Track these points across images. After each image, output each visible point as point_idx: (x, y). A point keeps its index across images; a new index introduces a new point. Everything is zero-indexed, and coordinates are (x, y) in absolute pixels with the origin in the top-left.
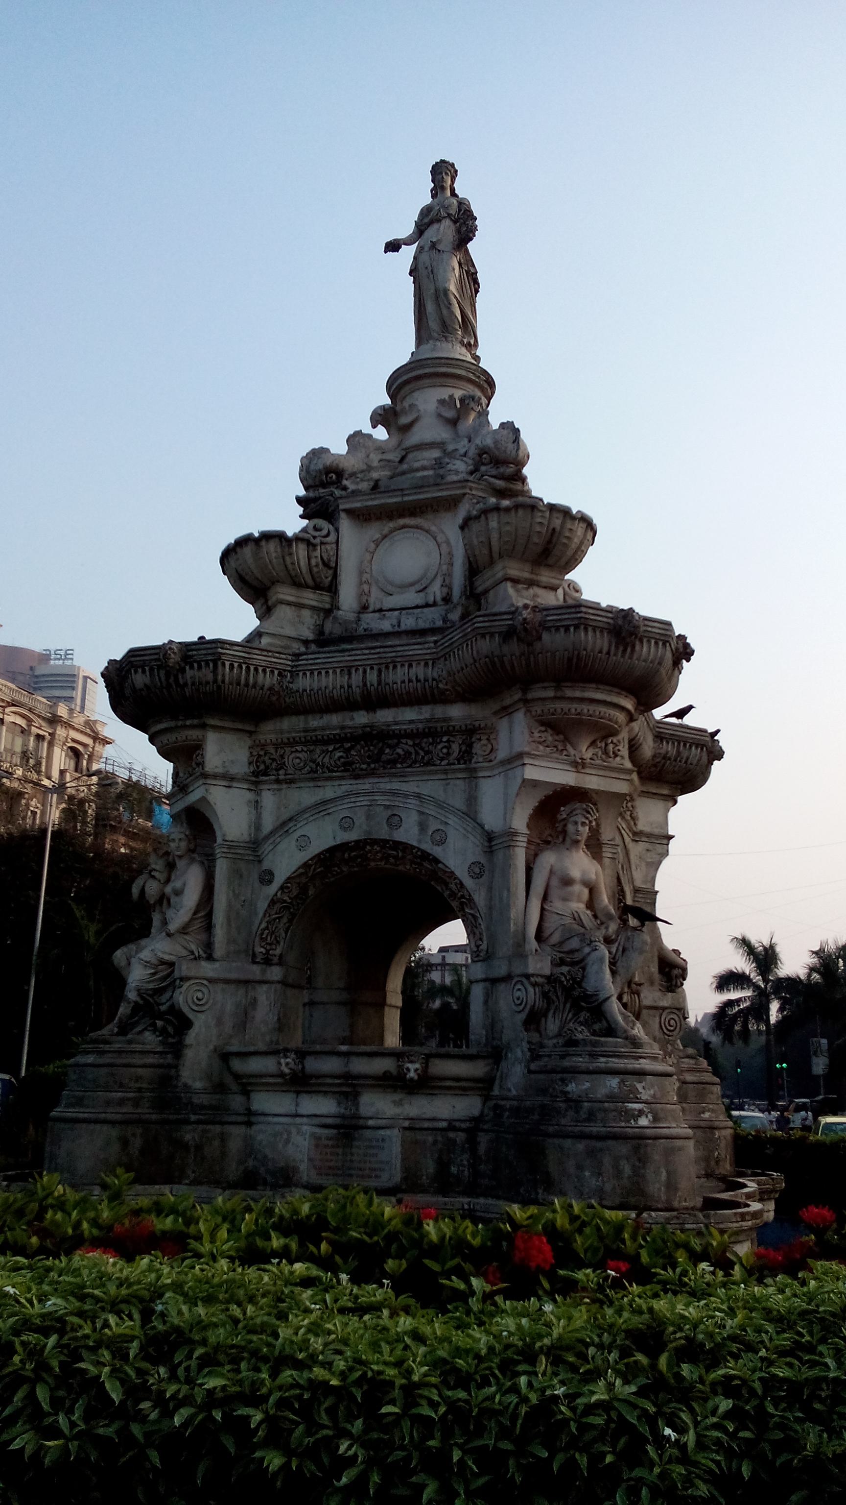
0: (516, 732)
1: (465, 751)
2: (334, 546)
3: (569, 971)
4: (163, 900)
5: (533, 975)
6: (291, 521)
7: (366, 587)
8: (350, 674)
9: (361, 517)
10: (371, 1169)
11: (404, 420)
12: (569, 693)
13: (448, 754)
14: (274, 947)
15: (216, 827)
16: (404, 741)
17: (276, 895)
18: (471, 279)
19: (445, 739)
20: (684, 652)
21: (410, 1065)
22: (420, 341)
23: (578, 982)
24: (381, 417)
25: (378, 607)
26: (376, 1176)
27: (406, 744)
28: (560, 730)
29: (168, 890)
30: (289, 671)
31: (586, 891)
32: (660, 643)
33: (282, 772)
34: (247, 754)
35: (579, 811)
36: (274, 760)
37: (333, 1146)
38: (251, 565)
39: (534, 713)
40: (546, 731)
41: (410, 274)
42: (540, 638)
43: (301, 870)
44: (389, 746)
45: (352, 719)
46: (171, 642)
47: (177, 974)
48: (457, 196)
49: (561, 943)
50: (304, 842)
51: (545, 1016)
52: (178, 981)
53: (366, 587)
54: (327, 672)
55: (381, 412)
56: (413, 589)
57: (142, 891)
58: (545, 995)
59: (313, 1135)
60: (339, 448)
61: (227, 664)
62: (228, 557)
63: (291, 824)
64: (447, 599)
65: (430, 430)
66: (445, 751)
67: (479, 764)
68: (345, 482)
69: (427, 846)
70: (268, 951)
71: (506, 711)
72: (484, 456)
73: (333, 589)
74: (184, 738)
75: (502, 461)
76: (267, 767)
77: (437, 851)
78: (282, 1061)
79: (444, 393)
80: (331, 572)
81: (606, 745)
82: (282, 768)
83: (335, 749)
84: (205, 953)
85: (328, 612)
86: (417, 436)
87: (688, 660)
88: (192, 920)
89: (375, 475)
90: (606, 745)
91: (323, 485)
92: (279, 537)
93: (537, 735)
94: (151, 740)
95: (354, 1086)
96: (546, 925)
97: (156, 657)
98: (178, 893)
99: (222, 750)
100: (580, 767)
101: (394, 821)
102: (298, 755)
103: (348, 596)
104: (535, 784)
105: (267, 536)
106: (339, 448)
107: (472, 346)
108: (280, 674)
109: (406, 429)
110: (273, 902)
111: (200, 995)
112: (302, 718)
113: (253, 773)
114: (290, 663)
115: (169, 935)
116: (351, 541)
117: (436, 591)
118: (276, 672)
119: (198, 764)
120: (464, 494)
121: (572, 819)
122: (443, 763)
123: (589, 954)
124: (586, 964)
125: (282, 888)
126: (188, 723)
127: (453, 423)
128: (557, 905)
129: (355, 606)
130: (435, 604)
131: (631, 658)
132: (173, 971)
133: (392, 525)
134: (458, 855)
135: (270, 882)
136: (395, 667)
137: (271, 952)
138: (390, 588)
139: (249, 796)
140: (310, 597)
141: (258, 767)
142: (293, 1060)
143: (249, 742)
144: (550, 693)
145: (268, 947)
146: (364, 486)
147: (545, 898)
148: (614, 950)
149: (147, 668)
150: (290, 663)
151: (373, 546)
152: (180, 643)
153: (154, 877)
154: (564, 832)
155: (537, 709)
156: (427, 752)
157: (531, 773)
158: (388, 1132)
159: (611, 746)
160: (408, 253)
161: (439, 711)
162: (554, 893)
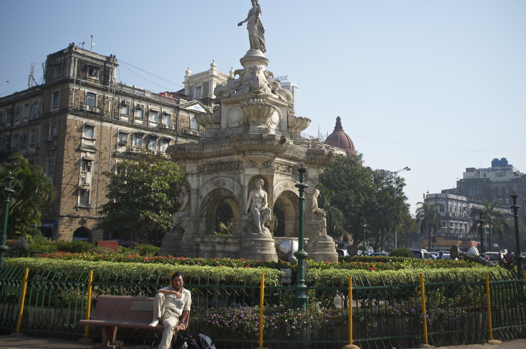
69: (231, 190)
101: (224, 184)
110: (202, 203)
130: (242, 126)
133: (233, 106)
160: (245, 25)
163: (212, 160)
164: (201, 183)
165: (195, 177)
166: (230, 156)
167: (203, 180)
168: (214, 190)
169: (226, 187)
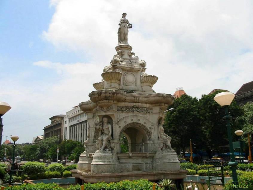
50: (125, 122)
77: (145, 125)
101: (139, 120)
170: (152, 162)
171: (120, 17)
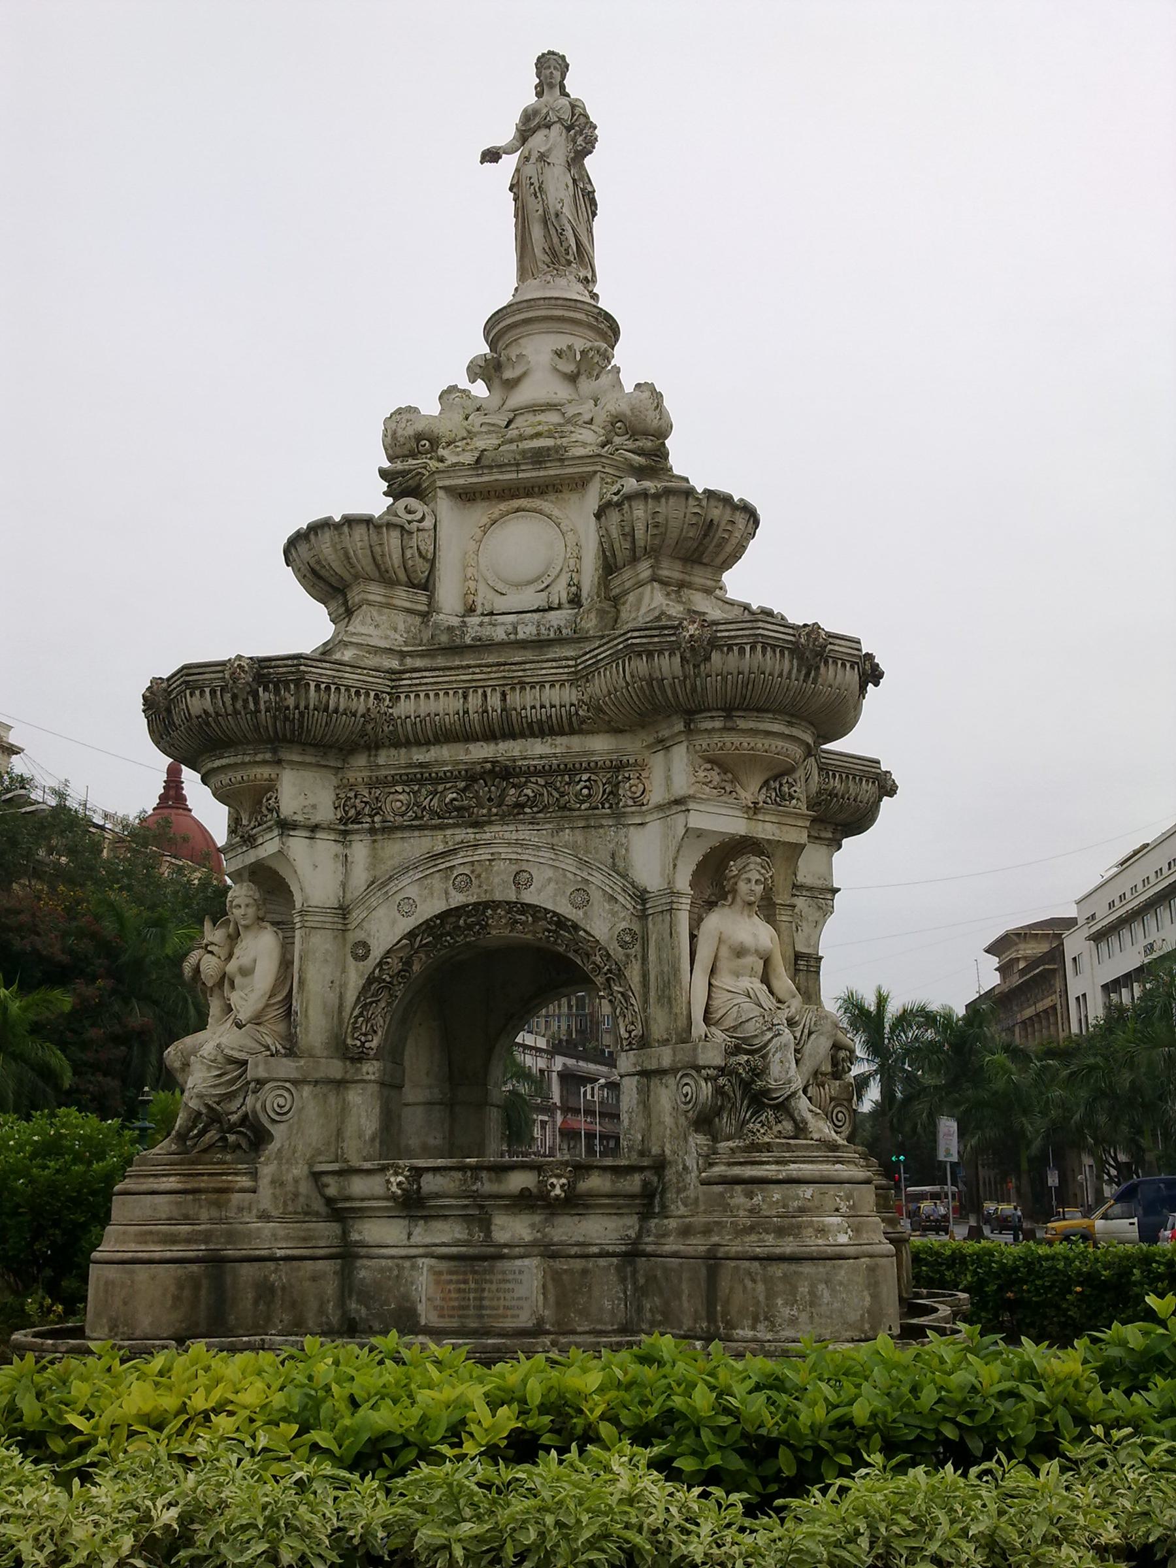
0: (674, 771)
1: (611, 793)
2: (432, 533)
3: (748, 1061)
4: (224, 981)
5: (704, 1068)
6: (374, 501)
7: (472, 584)
8: (465, 697)
9: (463, 497)
10: (506, 1308)
11: (508, 374)
12: (742, 724)
13: (589, 795)
14: (370, 1037)
15: (294, 889)
16: (533, 779)
17: (373, 972)
18: (587, 200)
19: (585, 777)
20: (871, 674)
21: (554, 1180)
22: (524, 273)
23: (759, 1073)
24: (478, 370)
25: (488, 609)
26: (513, 1316)
27: (537, 783)
28: (725, 769)
29: (232, 967)
30: (388, 693)
31: (761, 962)
32: (848, 665)
33: (377, 819)
34: (334, 797)
35: (752, 866)
36: (366, 803)
37: (458, 1282)
38: (325, 560)
39: (698, 748)
40: (712, 769)
41: (511, 189)
42: (708, 659)
43: (404, 941)
44: (514, 786)
45: (467, 751)
46: (239, 657)
47: (250, 1075)
48: (568, 96)
49: (735, 1028)
51: (718, 1114)
52: (253, 1085)
53: (472, 584)
54: (437, 695)
55: (483, 364)
56: (531, 590)
57: (197, 970)
58: (719, 1091)
59: (431, 1268)
60: (430, 407)
61: (312, 684)
62: (294, 547)
63: (392, 884)
64: (575, 601)
65: (543, 384)
66: (585, 791)
67: (629, 809)
68: (441, 452)
69: (565, 909)
70: (363, 1043)
71: (663, 745)
72: (619, 424)
73: (427, 586)
74: (252, 777)
75: (642, 436)
76: (358, 813)
78: (392, 1179)
79: (562, 342)
80: (427, 565)
81: (781, 785)
82: (378, 813)
83: (445, 789)
84: (284, 1048)
85: (425, 616)
86: (524, 395)
87: (876, 684)
88: (267, 1006)
89: (480, 443)
90: (781, 785)
91: (413, 455)
92: (367, 521)
93: (702, 774)
94: (205, 781)
95: (481, 1207)
96: (715, 1003)
97: (220, 675)
98: (246, 972)
99: (301, 791)
100: (751, 812)
101: (520, 880)
102: (401, 797)
103: (449, 596)
104: (700, 834)
105: (350, 521)
106: (430, 407)
107: (588, 282)
108: (377, 697)
109: (511, 385)
110: (370, 980)
111: (281, 1101)
112: (403, 751)
113: (341, 819)
114: (389, 683)
115: (240, 1026)
116: (453, 528)
117: (560, 592)
118: (372, 694)
119: (270, 811)
120: (595, 472)
121: (744, 876)
122: (583, 807)
123: (770, 1040)
124: (768, 1053)
125: (380, 964)
126: (259, 758)
127: (573, 378)
128: (724, 980)
129: (460, 609)
131: (815, 682)
132: (246, 1070)
133: (504, 506)
134: (603, 924)
135: (365, 957)
136: (523, 689)
137: (367, 1045)
138: (500, 586)
139: (338, 848)
140: (402, 597)
141: (346, 812)
142: (406, 1178)
143: (335, 781)
144: (718, 724)
145: (363, 1039)
146: (468, 458)
147: (713, 972)
148: (798, 1035)
149: (207, 690)
150: (389, 683)
151: (480, 533)
152: (251, 658)
153: (211, 952)
154: (734, 891)
155: (703, 742)
156: (562, 795)
157: (697, 820)
158: (527, 1262)
159: (785, 789)
160: (509, 163)
161: (576, 743)
162: (723, 965)
163: (444, 755)
164: (360, 876)
165: (326, 846)
166: (559, 740)
167: (375, 859)
168: (443, 916)
169: (530, 897)
170: (637, 1241)
171: (523, 93)
